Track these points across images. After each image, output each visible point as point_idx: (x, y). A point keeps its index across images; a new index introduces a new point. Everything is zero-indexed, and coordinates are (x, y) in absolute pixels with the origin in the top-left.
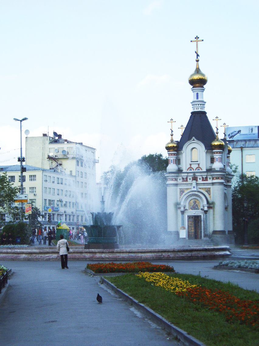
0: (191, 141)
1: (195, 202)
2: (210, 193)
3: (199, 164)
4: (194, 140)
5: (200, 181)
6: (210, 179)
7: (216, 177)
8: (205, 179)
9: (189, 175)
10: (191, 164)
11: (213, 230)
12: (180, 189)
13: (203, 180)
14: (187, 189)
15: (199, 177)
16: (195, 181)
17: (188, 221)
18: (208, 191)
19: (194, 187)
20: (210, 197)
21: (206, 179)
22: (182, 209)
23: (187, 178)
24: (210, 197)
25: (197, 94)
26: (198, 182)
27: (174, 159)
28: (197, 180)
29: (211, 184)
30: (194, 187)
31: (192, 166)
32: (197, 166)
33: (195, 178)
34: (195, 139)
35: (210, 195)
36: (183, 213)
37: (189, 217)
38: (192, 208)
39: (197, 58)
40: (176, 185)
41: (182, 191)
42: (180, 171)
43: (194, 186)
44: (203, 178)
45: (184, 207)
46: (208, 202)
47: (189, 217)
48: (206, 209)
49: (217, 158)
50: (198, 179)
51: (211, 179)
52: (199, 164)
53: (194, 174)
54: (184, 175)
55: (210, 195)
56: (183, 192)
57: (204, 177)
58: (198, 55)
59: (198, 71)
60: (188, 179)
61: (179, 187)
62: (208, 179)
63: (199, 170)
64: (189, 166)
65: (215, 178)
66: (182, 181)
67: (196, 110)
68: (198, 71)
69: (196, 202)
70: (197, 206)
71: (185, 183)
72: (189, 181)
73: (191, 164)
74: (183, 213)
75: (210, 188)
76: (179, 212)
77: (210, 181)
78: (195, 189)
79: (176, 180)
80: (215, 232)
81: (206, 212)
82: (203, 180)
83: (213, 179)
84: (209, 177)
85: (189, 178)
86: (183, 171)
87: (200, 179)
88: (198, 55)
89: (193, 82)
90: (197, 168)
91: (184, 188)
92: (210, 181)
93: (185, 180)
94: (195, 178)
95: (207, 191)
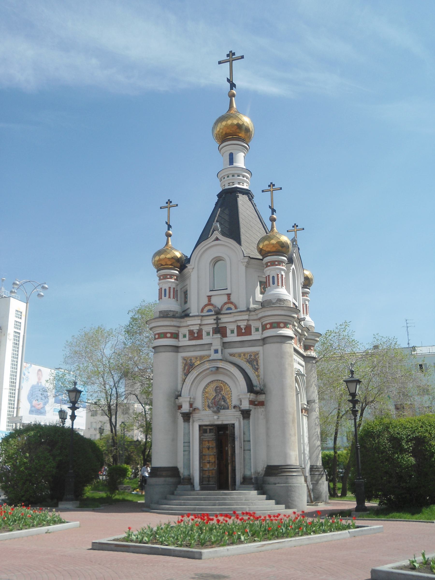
1: (218, 390)
2: (257, 364)
3: (229, 295)
4: (217, 239)
5: (232, 337)
6: (257, 330)
7: (271, 324)
8: (243, 331)
9: (205, 322)
10: (209, 297)
11: (266, 466)
12: (184, 359)
15: (230, 327)
16: (219, 336)
17: (201, 441)
18: (253, 360)
19: (216, 351)
20: (258, 376)
21: (248, 331)
22: (186, 408)
23: (200, 331)
24: (258, 376)
27: (170, 288)
28: (224, 335)
29: (261, 343)
30: (216, 351)
31: (214, 301)
32: (225, 299)
33: (220, 331)
34: (220, 237)
35: (257, 370)
36: (187, 417)
37: (203, 429)
38: (211, 405)
40: (176, 349)
43: (216, 348)
44: (239, 327)
45: (191, 405)
46: (251, 388)
48: (245, 405)
49: (273, 277)
50: (228, 332)
51: (260, 329)
52: (229, 295)
53: (217, 319)
54: (193, 323)
57: (243, 325)
60: (204, 334)
61: (181, 355)
63: (229, 309)
64: (206, 301)
65: (268, 326)
66: (190, 340)
67: (227, 187)
69: (221, 390)
70: (224, 399)
72: (206, 340)
73: (209, 297)
74: (187, 417)
77: (256, 336)
78: (219, 356)
79: (175, 336)
81: (246, 414)
83: (264, 328)
86: (191, 315)
87: (232, 332)
90: (225, 304)
91: (193, 357)
92: (256, 336)
93: (196, 335)
94: (220, 331)
95: (250, 362)
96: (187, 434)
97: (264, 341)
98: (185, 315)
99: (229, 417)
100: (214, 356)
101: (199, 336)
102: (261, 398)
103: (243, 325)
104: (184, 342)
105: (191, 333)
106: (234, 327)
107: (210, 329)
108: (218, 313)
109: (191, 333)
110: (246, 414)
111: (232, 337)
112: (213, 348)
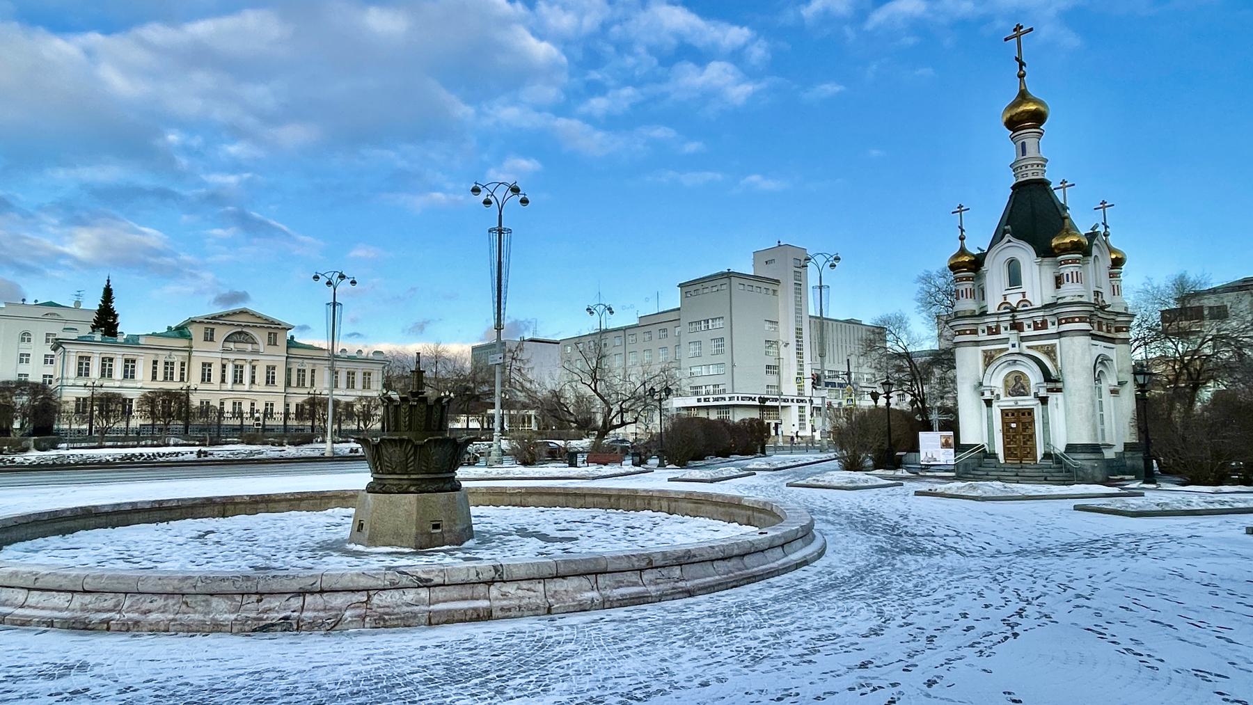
3: (1024, 294)
5: (1028, 332)
14: (1001, 350)
15: (1026, 323)
18: (1050, 352)
19: (1014, 346)
20: (1056, 366)
21: (1044, 325)
22: (988, 395)
23: (998, 327)
24: (1056, 366)
26: (1022, 334)
30: (1014, 346)
35: (1054, 360)
36: (989, 403)
37: (1005, 413)
40: (977, 343)
48: (1043, 393)
55: (1054, 360)
57: (1039, 320)
58: (1022, 64)
59: (1023, 96)
62: (1049, 324)
68: (1023, 96)
72: (1004, 334)
73: (1005, 297)
74: (989, 403)
75: (1054, 345)
78: (1016, 350)
79: (975, 332)
80: (1071, 448)
81: (1044, 401)
85: (1002, 325)
88: (1022, 64)
89: (1013, 124)
92: (1052, 329)
94: (1016, 326)
96: (990, 418)
97: (1060, 335)
98: (984, 314)
99: (1027, 402)
100: (1012, 350)
102: (1059, 385)
103: (1039, 320)
104: (983, 337)
106: (1030, 322)
108: (1014, 310)
110: (1044, 401)
111: (1028, 332)
112: (1011, 342)
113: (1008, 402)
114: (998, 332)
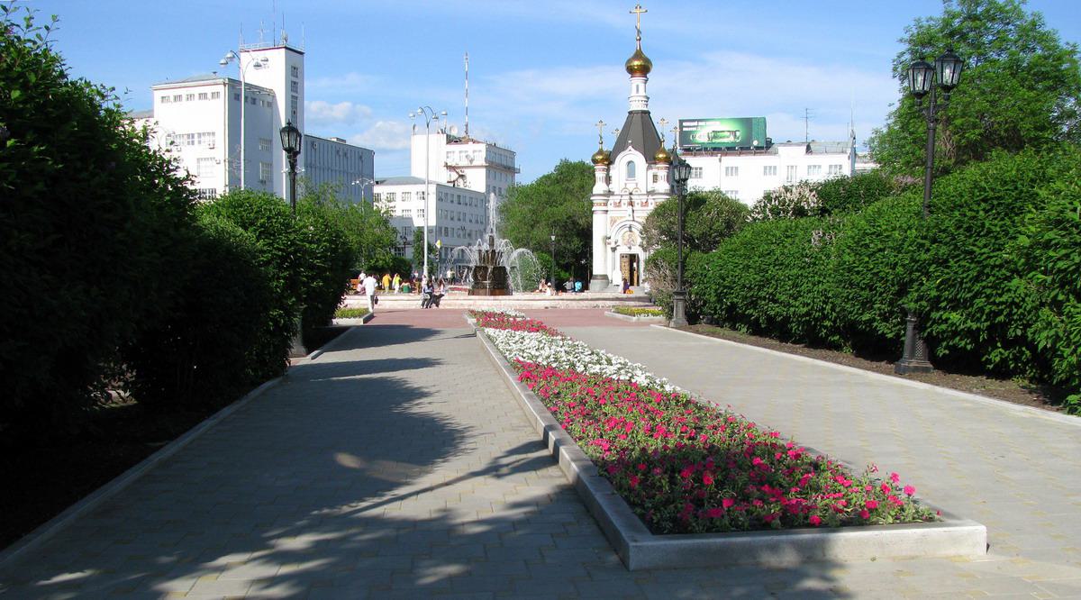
0: (626, 152)
3: (637, 184)
13: (642, 206)
22: (613, 245)
25: (638, 86)
32: (634, 186)
33: (631, 204)
34: (632, 149)
36: (614, 250)
37: (622, 256)
39: (638, 35)
41: (613, 221)
42: (610, 193)
45: (616, 243)
47: (622, 256)
53: (631, 199)
54: (617, 199)
56: (615, 221)
71: (617, 209)
74: (614, 250)
76: (609, 247)
79: (606, 205)
82: (642, 206)
84: (650, 201)
94: (631, 204)
101: (619, 206)
105: (615, 203)
106: (639, 201)
107: (626, 202)
109: (615, 203)
113: (623, 250)
114: (619, 206)
